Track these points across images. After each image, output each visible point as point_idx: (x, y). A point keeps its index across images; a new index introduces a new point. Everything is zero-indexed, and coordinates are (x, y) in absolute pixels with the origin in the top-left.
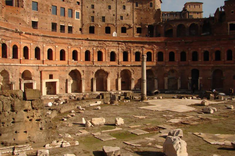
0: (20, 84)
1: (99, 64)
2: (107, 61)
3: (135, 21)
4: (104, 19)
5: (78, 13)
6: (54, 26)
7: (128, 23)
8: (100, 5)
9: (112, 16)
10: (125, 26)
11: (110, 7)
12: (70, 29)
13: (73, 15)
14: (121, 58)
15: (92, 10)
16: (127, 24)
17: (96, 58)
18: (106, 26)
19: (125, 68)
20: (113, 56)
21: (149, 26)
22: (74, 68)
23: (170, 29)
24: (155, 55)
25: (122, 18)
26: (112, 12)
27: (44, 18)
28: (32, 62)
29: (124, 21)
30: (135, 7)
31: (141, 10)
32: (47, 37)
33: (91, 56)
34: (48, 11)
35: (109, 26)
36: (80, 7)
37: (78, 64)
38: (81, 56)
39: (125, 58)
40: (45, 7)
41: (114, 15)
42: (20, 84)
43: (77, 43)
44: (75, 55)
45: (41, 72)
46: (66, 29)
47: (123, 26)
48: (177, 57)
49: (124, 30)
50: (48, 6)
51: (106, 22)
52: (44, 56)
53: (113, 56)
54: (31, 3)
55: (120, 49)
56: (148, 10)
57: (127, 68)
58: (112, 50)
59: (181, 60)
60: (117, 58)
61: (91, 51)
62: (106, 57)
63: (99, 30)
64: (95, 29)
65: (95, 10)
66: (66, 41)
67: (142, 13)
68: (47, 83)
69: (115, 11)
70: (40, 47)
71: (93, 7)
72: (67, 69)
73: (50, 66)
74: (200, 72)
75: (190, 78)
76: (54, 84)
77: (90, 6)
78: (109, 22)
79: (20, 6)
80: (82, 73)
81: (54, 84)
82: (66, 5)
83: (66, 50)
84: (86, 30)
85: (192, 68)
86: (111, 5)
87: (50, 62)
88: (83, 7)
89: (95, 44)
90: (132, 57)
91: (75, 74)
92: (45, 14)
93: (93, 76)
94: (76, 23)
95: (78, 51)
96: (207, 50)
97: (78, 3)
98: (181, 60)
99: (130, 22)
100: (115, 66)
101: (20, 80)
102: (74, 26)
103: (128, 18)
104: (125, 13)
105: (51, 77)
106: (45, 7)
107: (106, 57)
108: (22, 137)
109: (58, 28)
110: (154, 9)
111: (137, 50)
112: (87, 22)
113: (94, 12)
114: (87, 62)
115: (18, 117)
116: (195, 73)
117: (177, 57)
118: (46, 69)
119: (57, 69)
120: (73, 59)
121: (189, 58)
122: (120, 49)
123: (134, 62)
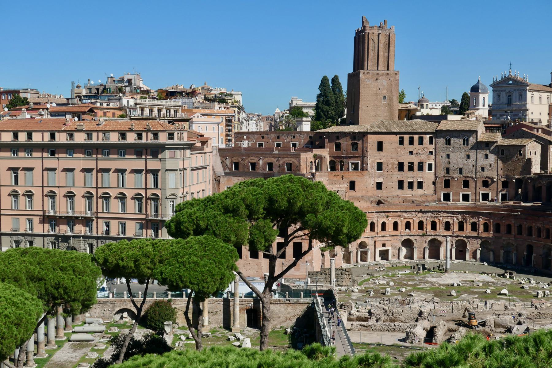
0: (357, 252)
1: (433, 233)
2: (441, 230)
3: (501, 172)
4: (461, 170)
5: (430, 166)
6: (401, 185)
7: (491, 176)
8: (457, 154)
9: (471, 167)
10: (487, 179)
11: (468, 157)
12: (420, 185)
13: (424, 168)
14: (456, 228)
15: (447, 160)
16: (489, 178)
17: (429, 227)
18: (464, 179)
19: (459, 238)
20: (448, 226)
21: (516, 179)
22: (407, 237)
23: (539, 185)
24: (492, 226)
25: (483, 169)
26: (471, 162)
27: (389, 177)
28: (367, 234)
29: (486, 173)
32: (381, 212)
33: (425, 226)
34: (394, 169)
35: (467, 179)
36: (433, 156)
37: (411, 234)
38: (414, 226)
39: (461, 228)
40: (390, 166)
41: (473, 166)
42: (357, 252)
43: (410, 215)
44: (408, 225)
45: (375, 242)
46: (415, 185)
47: (484, 179)
48: (514, 230)
50: (394, 163)
51: (464, 175)
52: (378, 228)
53: (448, 226)
54: (376, 164)
55: (455, 218)
56: (517, 159)
57: (462, 238)
58: (447, 220)
59: (518, 234)
60: (452, 228)
61: (425, 221)
62: (440, 228)
63: (455, 183)
65: (451, 161)
66: (399, 213)
68: (380, 251)
69: (475, 160)
70: (374, 221)
71: (448, 156)
72: (399, 238)
73: (384, 236)
74: (534, 248)
75: (525, 253)
76: (387, 251)
77: (445, 155)
78: (467, 175)
79: (365, 168)
80: (415, 242)
81: (387, 251)
82: (415, 158)
83: (399, 221)
84: (440, 184)
85: (527, 244)
86: (470, 154)
87: (383, 233)
88: (437, 156)
89: (429, 214)
90: (468, 228)
91: (408, 244)
92: (391, 173)
93: (426, 245)
94: (428, 176)
95: (411, 221)
97: (431, 153)
98: (518, 234)
99: (493, 174)
101: (357, 249)
102: (425, 181)
103: (491, 170)
104: (487, 163)
105: (384, 245)
106: (390, 166)
107: (440, 228)
108: (344, 283)
109: (406, 185)
110: (524, 158)
111: (473, 220)
112: (442, 173)
113: (449, 163)
114: (420, 231)
115: (343, 277)
116: (530, 249)
117: (514, 230)
118: (380, 239)
119: (390, 238)
120: (406, 228)
121: (525, 232)
122: (455, 218)
123: (469, 232)
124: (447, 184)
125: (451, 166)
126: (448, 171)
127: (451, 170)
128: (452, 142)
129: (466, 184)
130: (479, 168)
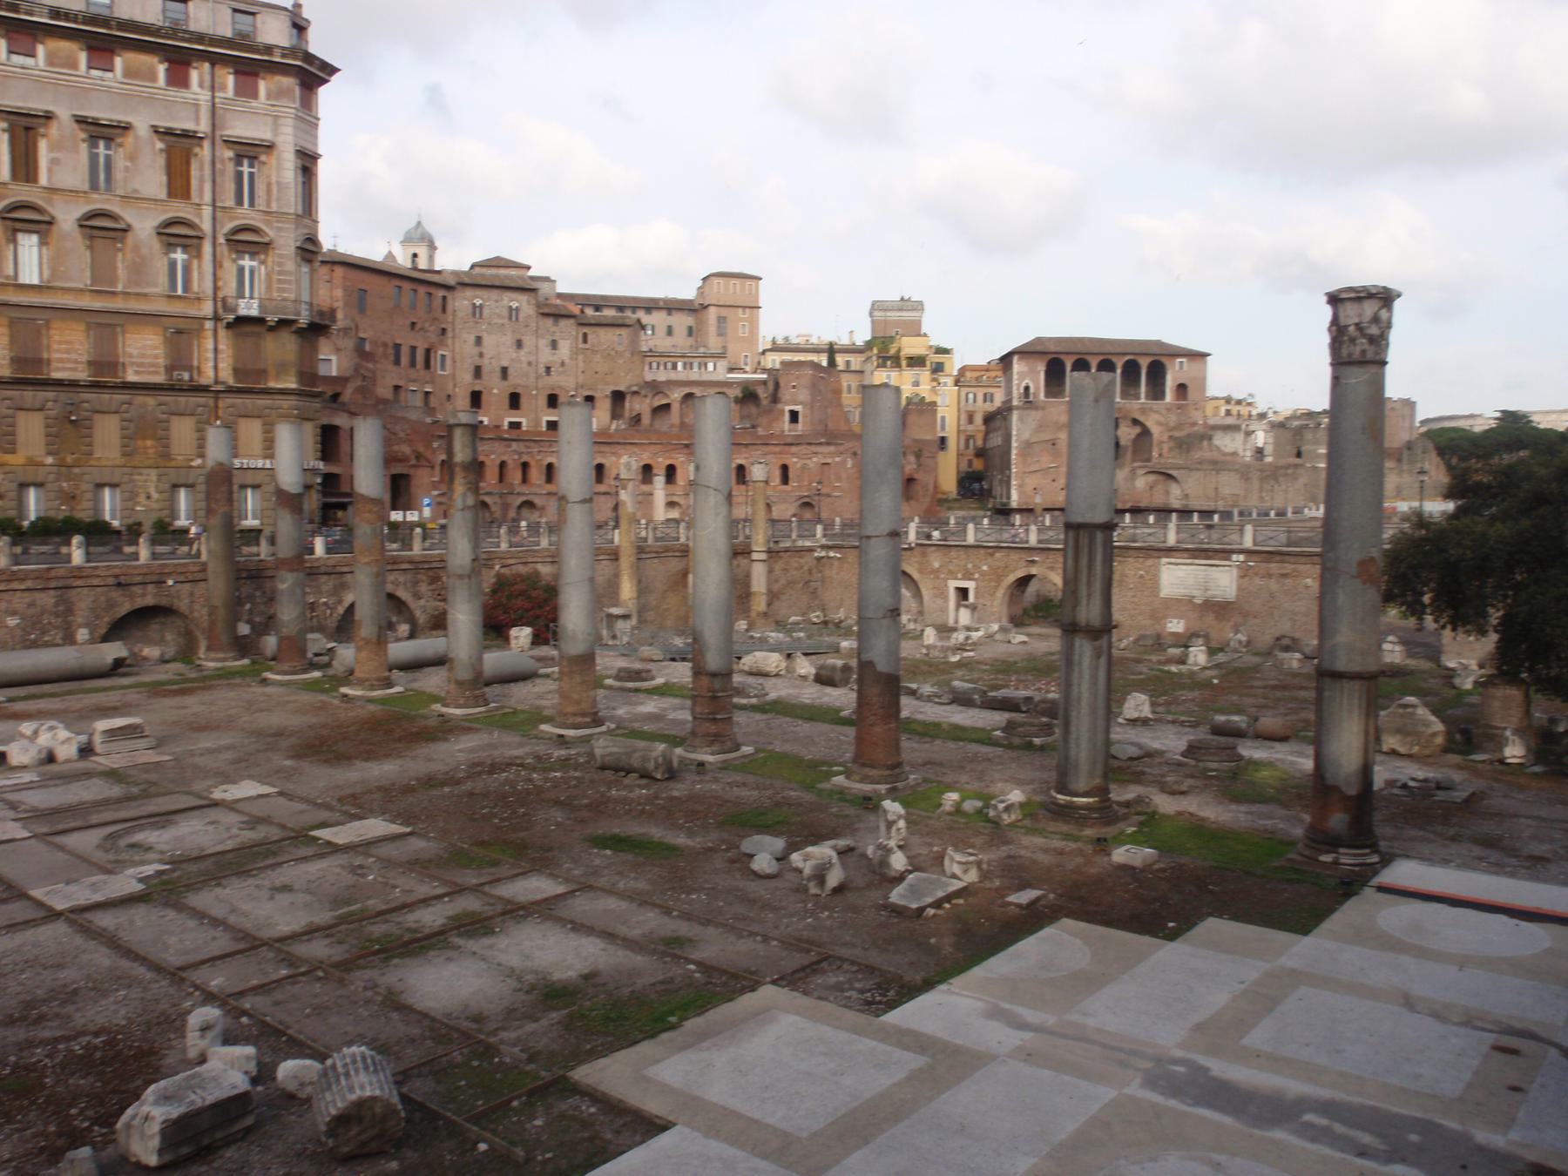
1: (524, 489)
4: (504, 372)
9: (525, 365)
11: (519, 344)
15: (476, 350)
25: (548, 369)
30: (581, 345)
31: (594, 352)
41: (530, 364)
49: (553, 401)
64: (484, 397)
67: (598, 358)
71: (479, 341)
77: (472, 339)
78: (519, 381)
84: (463, 401)
96: (742, 462)
104: (555, 358)
112: (466, 377)
113: (481, 355)
124: (476, 399)
125: (485, 363)
126: (478, 372)
127: (485, 370)
128: (486, 312)
129: (515, 401)
130: (542, 370)
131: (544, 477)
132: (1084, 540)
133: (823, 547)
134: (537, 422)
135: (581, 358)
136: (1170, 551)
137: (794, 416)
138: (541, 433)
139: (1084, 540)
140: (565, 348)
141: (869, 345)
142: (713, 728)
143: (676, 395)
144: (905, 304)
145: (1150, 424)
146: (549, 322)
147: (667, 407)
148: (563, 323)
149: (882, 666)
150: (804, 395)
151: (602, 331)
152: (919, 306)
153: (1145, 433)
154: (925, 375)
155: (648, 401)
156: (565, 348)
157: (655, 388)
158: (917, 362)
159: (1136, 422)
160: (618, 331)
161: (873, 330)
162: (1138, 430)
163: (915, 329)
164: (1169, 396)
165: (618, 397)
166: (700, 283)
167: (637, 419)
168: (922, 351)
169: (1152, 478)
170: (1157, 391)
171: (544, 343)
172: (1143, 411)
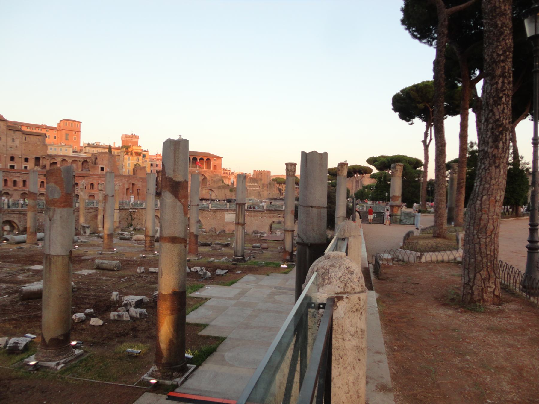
19: (24, 192)
41: (4, 146)
49: (12, 159)
58: (15, 179)
100: (17, 190)
107: (10, 184)
131: (12, 184)
132: (240, 207)
133: (131, 209)
134: (6, 165)
135: (23, 145)
136: (227, 210)
137: (102, 169)
138: (22, 170)
139: (240, 207)
140: (17, 142)
141: (122, 147)
142: (150, 249)
143: (59, 160)
144: (133, 136)
145: (206, 176)
146: (12, 132)
147: (56, 163)
148: (17, 133)
149: (195, 233)
150: (106, 162)
151: (32, 137)
152: (137, 137)
153: (205, 178)
154: (141, 158)
155: (49, 161)
156: (17, 142)
157: (51, 157)
158: (138, 154)
159: (202, 175)
160: (38, 137)
161: (122, 143)
162: (203, 177)
163: (136, 143)
164: (212, 169)
165: (37, 159)
166: (59, 122)
167: (44, 167)
168: (139, 151)
169: (207, 191)
170: (208, 167)
171: (9, 139)
172: (205, 172)
